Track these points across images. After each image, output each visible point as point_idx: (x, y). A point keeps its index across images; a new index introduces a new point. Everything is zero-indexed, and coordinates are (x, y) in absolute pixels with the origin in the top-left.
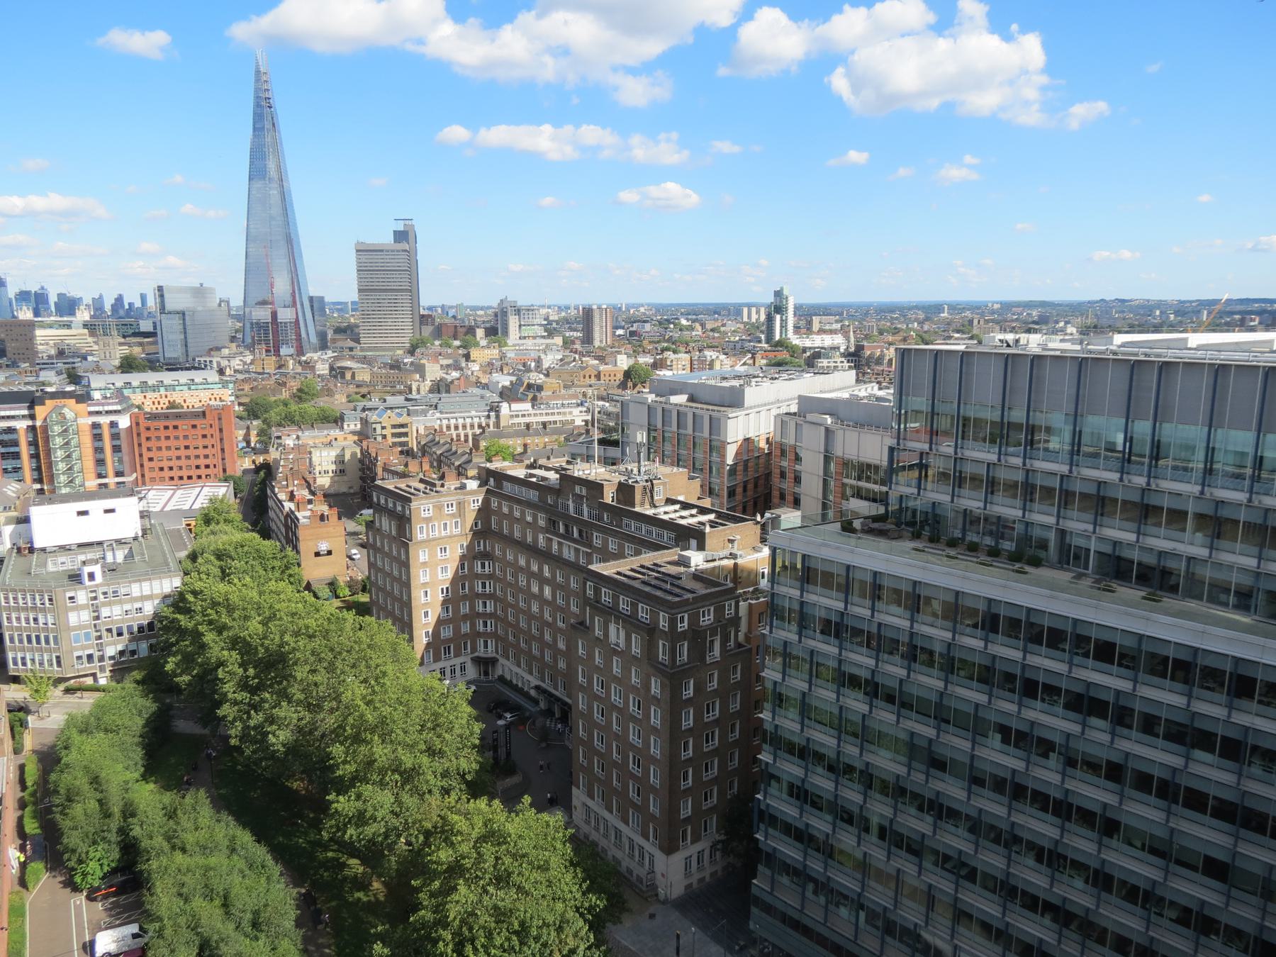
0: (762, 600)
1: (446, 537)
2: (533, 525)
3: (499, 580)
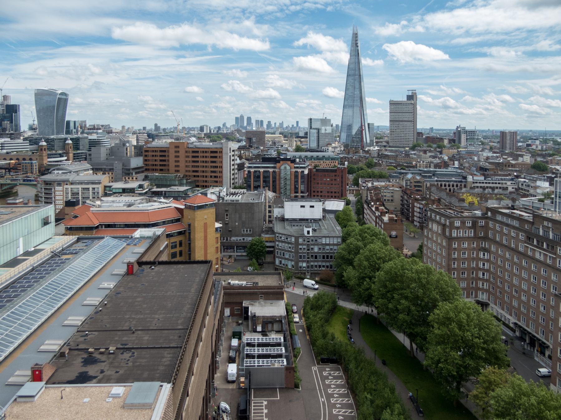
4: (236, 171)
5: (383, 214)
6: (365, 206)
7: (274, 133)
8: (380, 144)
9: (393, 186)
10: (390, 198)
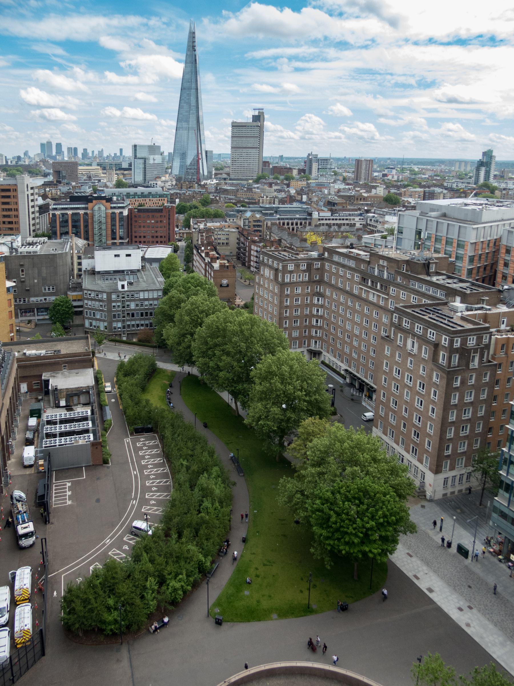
0: (504, 336)
1: (299, 282)
2: (351, 280)
3: (327, 309)
4: (37, 215)
5: (214, 259)
6: (195, 252)
7: (90, 165)
8: (219, 176)
9: (229, 226)
10: (225, 242)
